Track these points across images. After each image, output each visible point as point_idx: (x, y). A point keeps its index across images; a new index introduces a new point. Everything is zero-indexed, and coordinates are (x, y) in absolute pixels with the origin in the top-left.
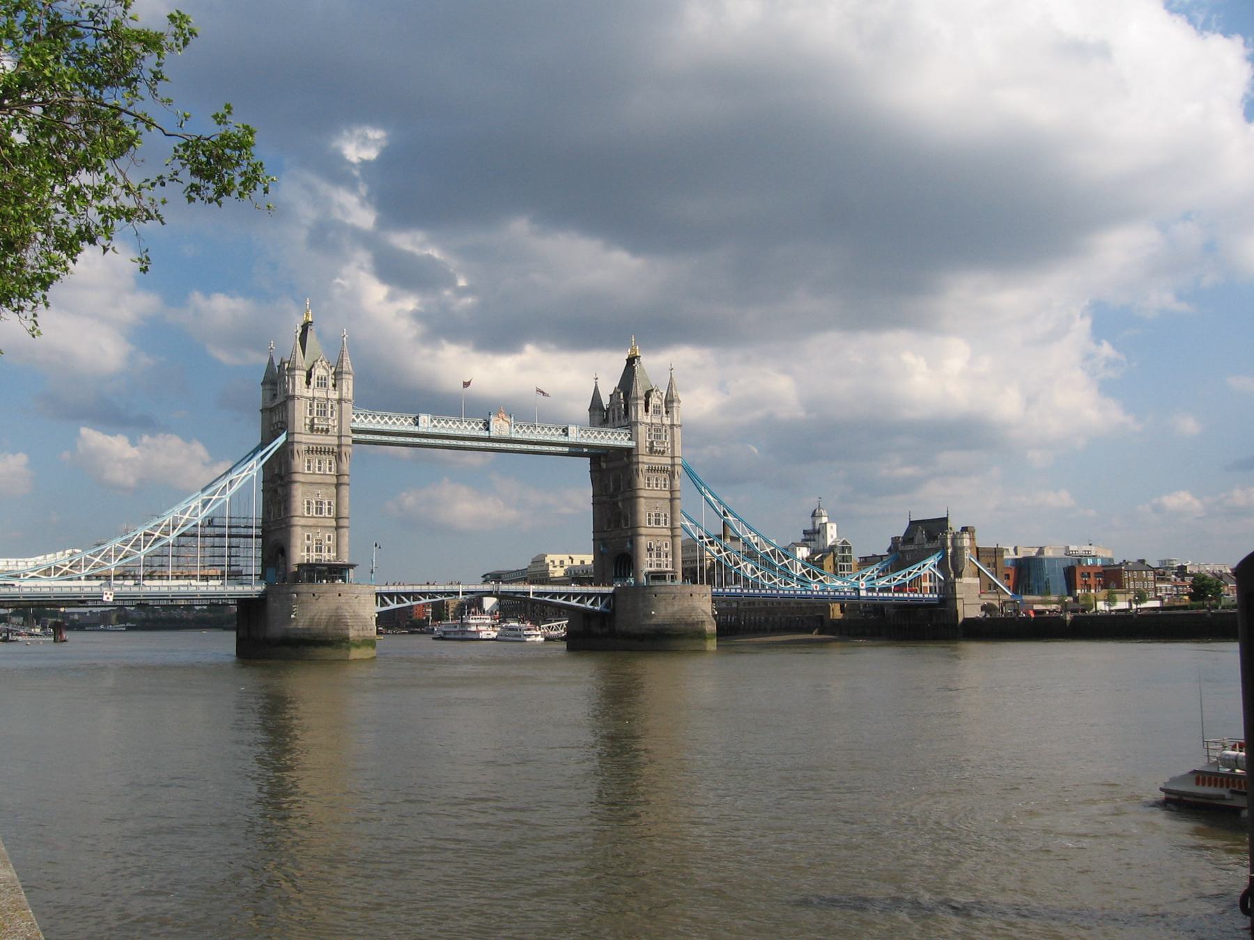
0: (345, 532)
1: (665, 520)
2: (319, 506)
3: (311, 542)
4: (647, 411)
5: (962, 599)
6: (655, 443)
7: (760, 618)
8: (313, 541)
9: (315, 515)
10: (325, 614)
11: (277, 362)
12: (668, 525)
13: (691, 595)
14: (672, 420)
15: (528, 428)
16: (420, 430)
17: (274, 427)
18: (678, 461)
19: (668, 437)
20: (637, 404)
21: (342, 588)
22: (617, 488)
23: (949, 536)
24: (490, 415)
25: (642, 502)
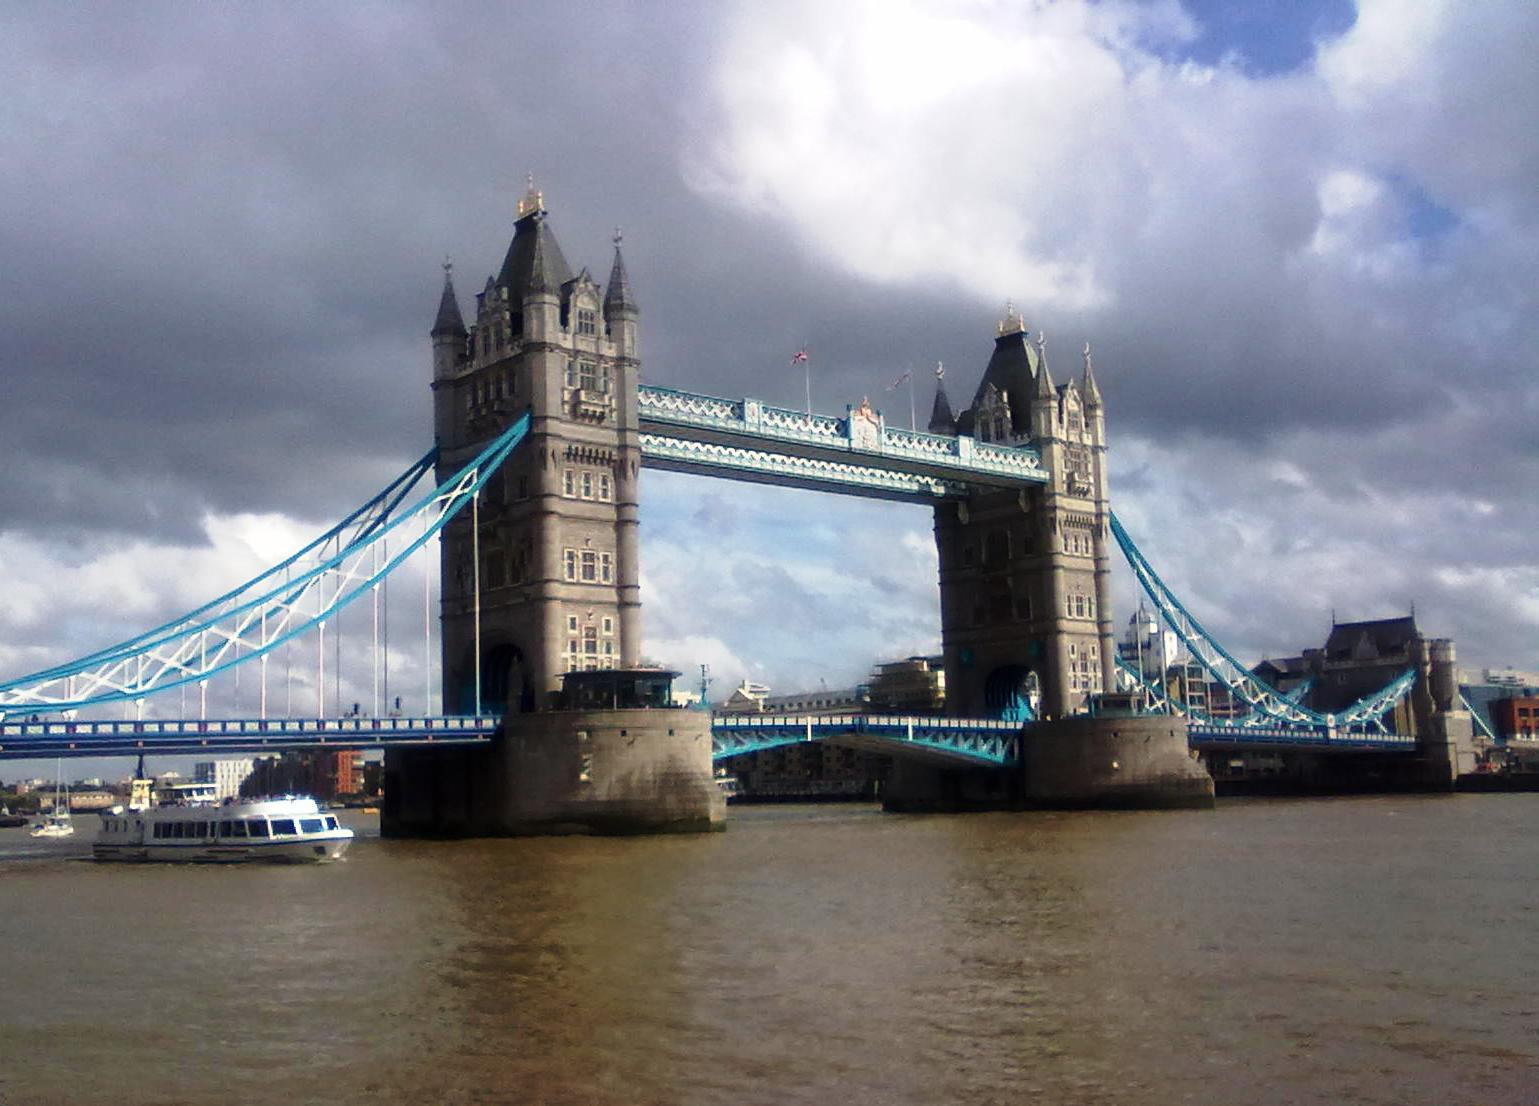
0: (632, 610)
3: (575, 632)
4: (1061, 420)
5: (1452, 743)
6: (1076, 475)
8: (581, 633)
10: (649, 771)
12: (1094, 617)
13: (1172, 733)
14: (1095, 438)
16: (747, 429)
17: (479, 411)
18: (1105, 508)
20: (1050, 407)
24: (849, 408)
25: (1060, 573)
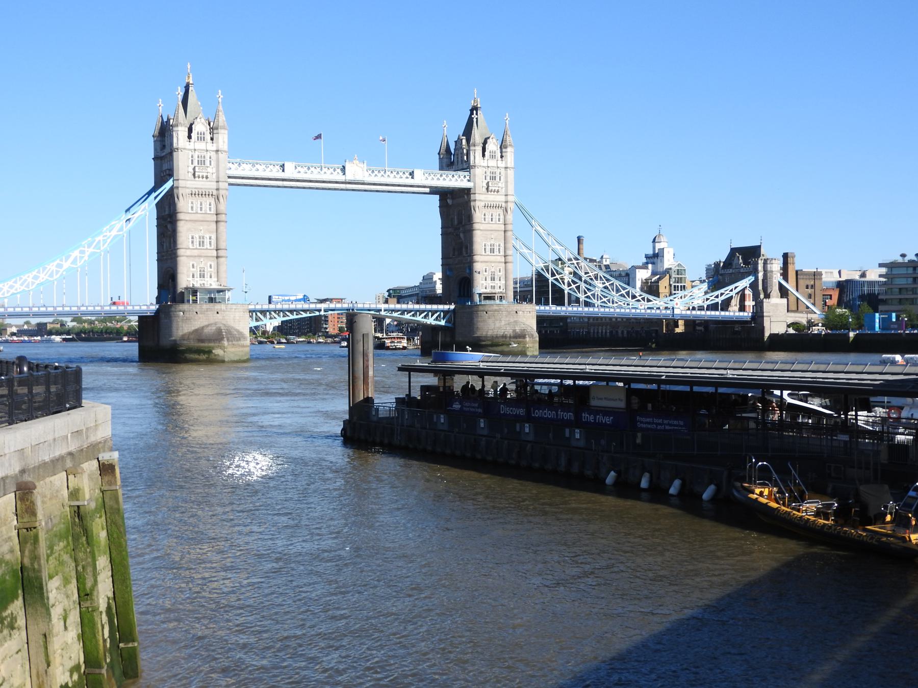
0: (221, 260)
1: (499, 249)
2: (202, 240)
3: (195, 269)
4: (484, 155)
7: (606, 332)
9: (198, 247)
11: (165, 120)
12: (502, 253)
14: (506, 163)
15: (379, 172)
18: (510, 198)
19: (502, 178)
21: (219, 307)
22: (460, 222)
23: (760, 261)
